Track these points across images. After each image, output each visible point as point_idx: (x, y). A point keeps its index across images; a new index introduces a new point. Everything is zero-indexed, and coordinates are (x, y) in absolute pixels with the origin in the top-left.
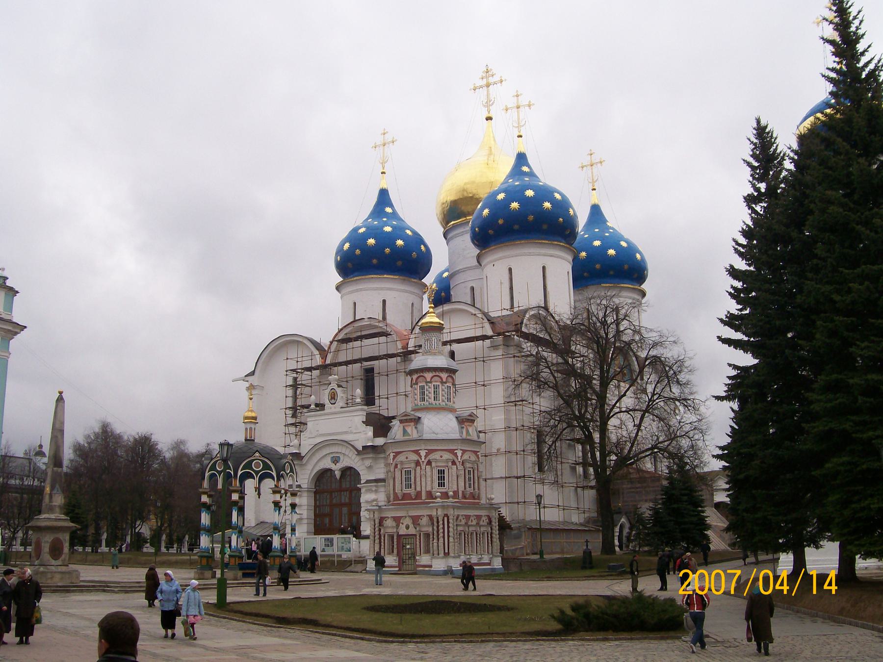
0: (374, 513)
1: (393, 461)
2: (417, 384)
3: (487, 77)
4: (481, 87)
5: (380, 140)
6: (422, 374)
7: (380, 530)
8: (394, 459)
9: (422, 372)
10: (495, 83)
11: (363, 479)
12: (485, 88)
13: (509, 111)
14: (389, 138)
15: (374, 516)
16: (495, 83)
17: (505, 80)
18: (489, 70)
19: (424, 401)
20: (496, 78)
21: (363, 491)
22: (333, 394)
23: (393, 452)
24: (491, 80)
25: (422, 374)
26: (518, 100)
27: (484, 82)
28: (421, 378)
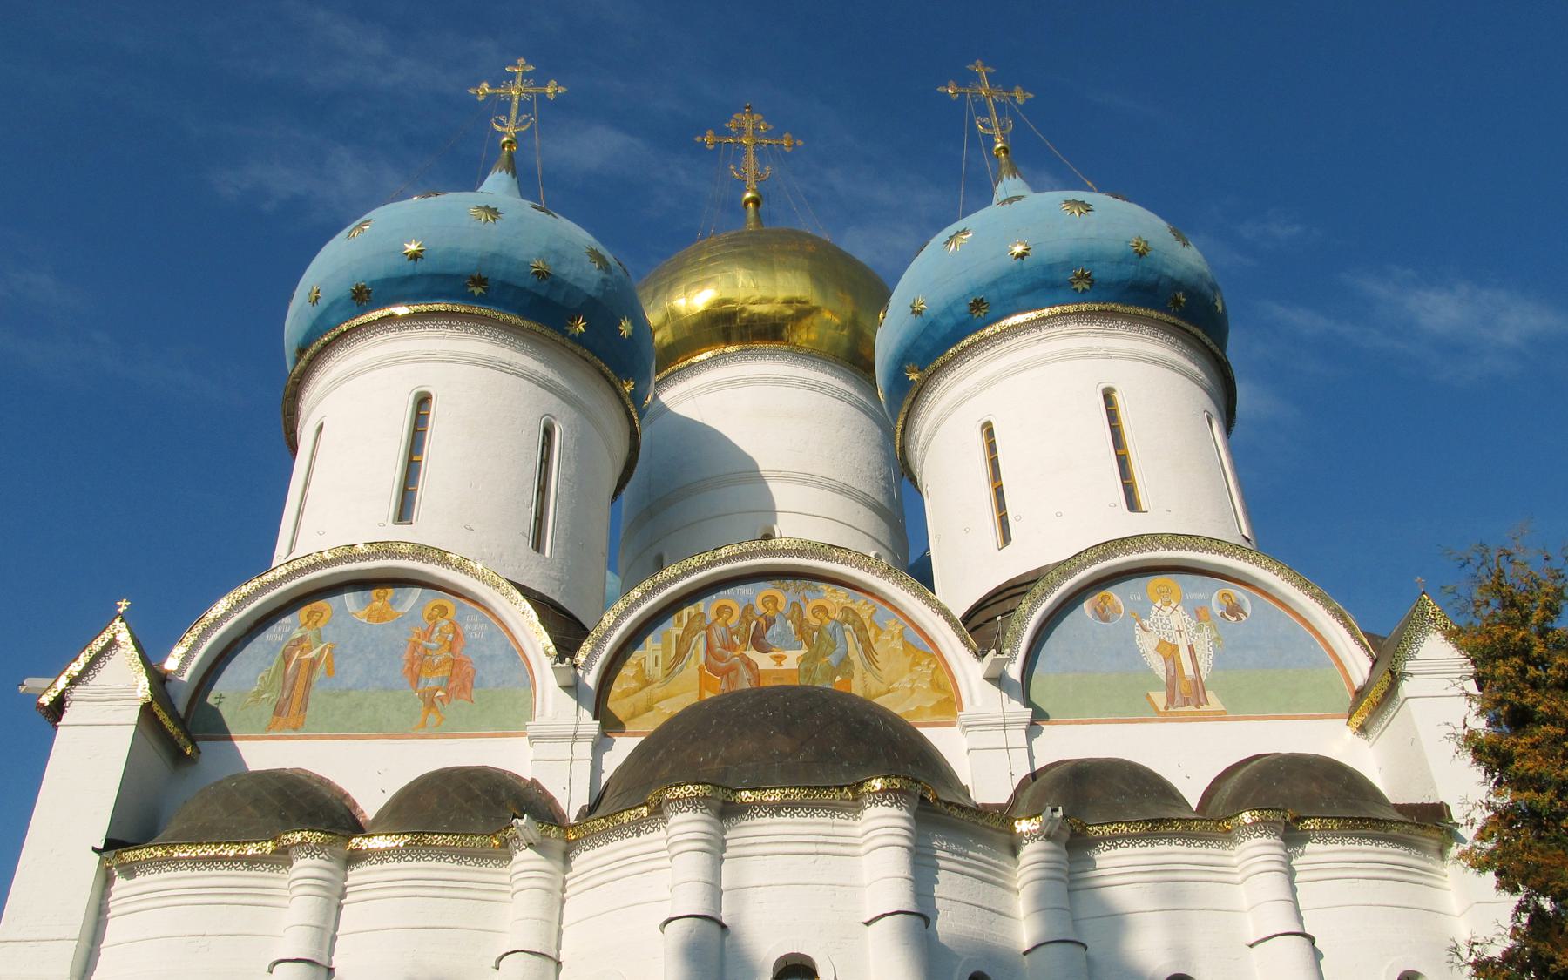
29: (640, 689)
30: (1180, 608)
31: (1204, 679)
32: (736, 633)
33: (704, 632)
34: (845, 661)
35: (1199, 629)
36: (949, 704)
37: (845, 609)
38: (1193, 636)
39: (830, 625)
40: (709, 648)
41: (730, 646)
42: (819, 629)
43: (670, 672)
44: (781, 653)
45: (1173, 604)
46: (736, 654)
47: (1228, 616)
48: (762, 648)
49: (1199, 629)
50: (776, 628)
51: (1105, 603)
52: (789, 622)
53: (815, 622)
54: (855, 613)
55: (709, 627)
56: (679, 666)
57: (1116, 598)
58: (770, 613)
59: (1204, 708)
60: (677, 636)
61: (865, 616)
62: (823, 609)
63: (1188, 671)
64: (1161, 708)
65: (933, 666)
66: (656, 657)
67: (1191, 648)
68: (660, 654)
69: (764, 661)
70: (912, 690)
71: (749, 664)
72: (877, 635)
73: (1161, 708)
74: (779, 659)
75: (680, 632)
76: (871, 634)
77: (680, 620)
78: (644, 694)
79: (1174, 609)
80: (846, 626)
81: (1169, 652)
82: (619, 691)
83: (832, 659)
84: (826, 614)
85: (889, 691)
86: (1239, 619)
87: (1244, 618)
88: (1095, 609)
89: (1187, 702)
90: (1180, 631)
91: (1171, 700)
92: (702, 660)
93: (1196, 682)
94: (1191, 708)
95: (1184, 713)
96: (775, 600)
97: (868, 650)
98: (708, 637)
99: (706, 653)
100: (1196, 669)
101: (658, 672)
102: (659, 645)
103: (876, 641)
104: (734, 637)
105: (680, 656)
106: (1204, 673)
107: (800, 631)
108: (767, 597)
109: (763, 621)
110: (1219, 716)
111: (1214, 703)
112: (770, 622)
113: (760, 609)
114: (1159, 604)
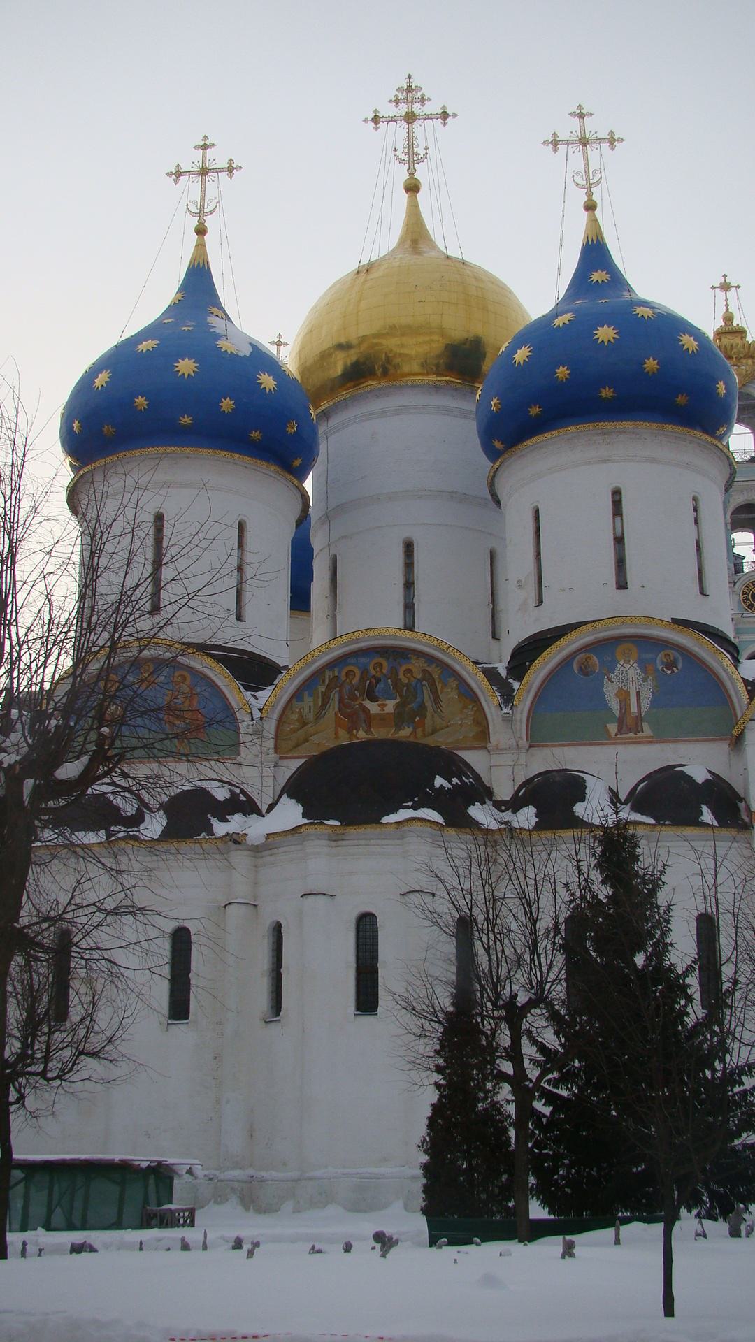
3: (410, 102)
4: (393, 119)
5: (192, 160)
10: (428, 117)
12: (404, 124)
13: (562, 148)
14: (217, 158)
16: (428, 117)
17: (455, 115)
18: (413, 87)
20: (432, 108)
24: (417, 108)
26: (583, 127)
27: (403, 108)
29: (301, 728)
30: (635, 665)
31: (643, 714)
32: (357, 689)
33: (338, 689)
34: (422, 707)
35: (645, 680)
36: (482, 737)
37: (424, 671)
38: (641, 685)
39: (414, 682)
40: (341, 700)
41: (353, 698)
42: (408, 685)
43: (318, 717)
44: (384, 702)
45: (631, 663)
46: (356, 703)
47: (665, 670)
48: (373, 699)
49: (645, 680)
50: (381, 685)
51: (588, 662)
52: (389, 681)
53: (405, 680)
54: (430, 674)
55: (341, 686)
56: (323, 712)
57: (595, 658)
58: (378, 675)
59: (641, 734)
60: (322, 692)
61: (435, 675)
62: (409, 671)
63: (634, 709)
64: (613, 735)
65: (475, 709)
66: (310, 707)
67: (638, 694)
68: (312, 704)
69: (373, 708)
70: (461, 725)
71: (365, 710)
72: (442, 688)
73: (613, 735)
74: (382, 706)
75: (324, 690)
76: (439, 688)
77: (324, 681)
78: (301, 732)
79: (632, 666)
80: (425, 683)
81: (624, 697)
82: (289, 729)
83: (414, 705)
84: (412, 675)
85: (447, 727)
86: (673, 672)
87: (676, 671)
88: (581, 667)
89: (630, 730)
90: (633, 681)
91: (620, 730)
92: (337, 709)
93: (637, 717)
94: (632, 735)
95: (626, 738)
96: (381, 665)
97: (437, 699)
98: (340, 692)
99: (339, 703)
100: (639, 707)
101: (311, 717)
102: (311, 699)
103: (441, 693)
104: (356, 692)
105: (324, 706)
106: (644, 710)
107: (396, 686)
108: (377, 663)
109: (373, 680)
110: (648, 741)
111: (647, 731)
112: (378, 681)
113: (372, 672)
114: (622, 663)
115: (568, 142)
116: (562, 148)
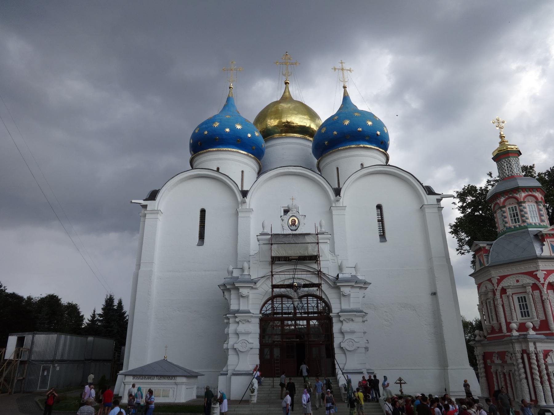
0: (535, 344)
1: (545, 281)
2: (524, 202)
6: (530, 193)
7: (547, 369)
8: (545, 279)
9: (531, 192)
11: (335, 309)
15: (536, 348)
19: (519, 222)
21: (334, 320)
22: (293, 220)
23: (542, 270)
25: (530, 193)
26: (342, 65)
28: (529, 197)
115: (339, 69)
116: (337, 71)
